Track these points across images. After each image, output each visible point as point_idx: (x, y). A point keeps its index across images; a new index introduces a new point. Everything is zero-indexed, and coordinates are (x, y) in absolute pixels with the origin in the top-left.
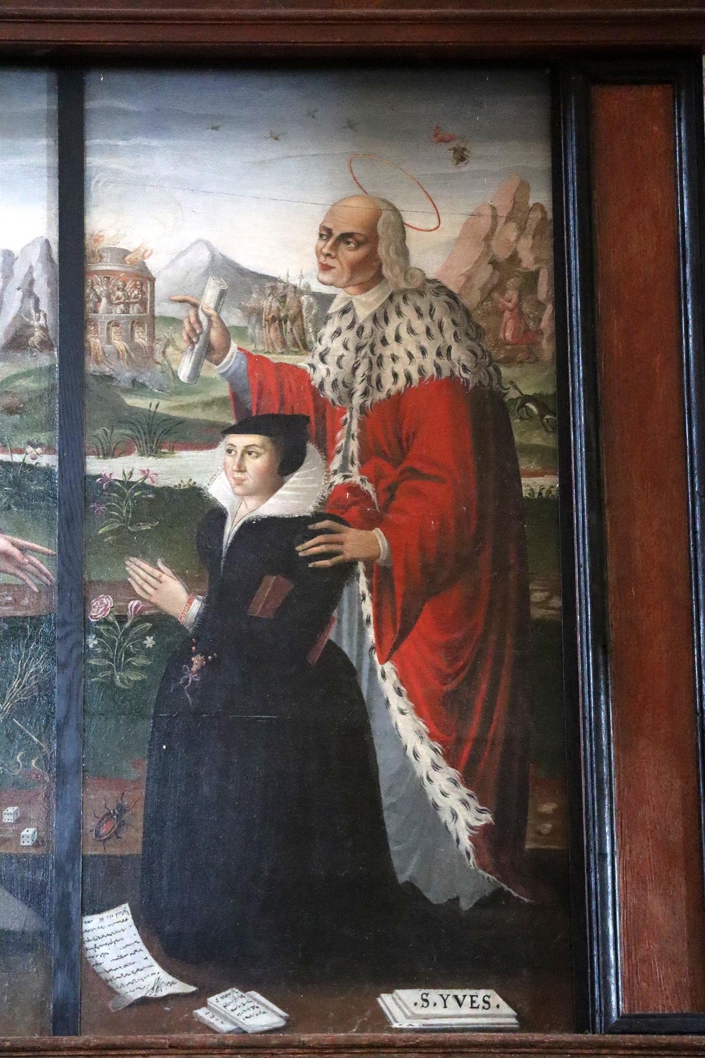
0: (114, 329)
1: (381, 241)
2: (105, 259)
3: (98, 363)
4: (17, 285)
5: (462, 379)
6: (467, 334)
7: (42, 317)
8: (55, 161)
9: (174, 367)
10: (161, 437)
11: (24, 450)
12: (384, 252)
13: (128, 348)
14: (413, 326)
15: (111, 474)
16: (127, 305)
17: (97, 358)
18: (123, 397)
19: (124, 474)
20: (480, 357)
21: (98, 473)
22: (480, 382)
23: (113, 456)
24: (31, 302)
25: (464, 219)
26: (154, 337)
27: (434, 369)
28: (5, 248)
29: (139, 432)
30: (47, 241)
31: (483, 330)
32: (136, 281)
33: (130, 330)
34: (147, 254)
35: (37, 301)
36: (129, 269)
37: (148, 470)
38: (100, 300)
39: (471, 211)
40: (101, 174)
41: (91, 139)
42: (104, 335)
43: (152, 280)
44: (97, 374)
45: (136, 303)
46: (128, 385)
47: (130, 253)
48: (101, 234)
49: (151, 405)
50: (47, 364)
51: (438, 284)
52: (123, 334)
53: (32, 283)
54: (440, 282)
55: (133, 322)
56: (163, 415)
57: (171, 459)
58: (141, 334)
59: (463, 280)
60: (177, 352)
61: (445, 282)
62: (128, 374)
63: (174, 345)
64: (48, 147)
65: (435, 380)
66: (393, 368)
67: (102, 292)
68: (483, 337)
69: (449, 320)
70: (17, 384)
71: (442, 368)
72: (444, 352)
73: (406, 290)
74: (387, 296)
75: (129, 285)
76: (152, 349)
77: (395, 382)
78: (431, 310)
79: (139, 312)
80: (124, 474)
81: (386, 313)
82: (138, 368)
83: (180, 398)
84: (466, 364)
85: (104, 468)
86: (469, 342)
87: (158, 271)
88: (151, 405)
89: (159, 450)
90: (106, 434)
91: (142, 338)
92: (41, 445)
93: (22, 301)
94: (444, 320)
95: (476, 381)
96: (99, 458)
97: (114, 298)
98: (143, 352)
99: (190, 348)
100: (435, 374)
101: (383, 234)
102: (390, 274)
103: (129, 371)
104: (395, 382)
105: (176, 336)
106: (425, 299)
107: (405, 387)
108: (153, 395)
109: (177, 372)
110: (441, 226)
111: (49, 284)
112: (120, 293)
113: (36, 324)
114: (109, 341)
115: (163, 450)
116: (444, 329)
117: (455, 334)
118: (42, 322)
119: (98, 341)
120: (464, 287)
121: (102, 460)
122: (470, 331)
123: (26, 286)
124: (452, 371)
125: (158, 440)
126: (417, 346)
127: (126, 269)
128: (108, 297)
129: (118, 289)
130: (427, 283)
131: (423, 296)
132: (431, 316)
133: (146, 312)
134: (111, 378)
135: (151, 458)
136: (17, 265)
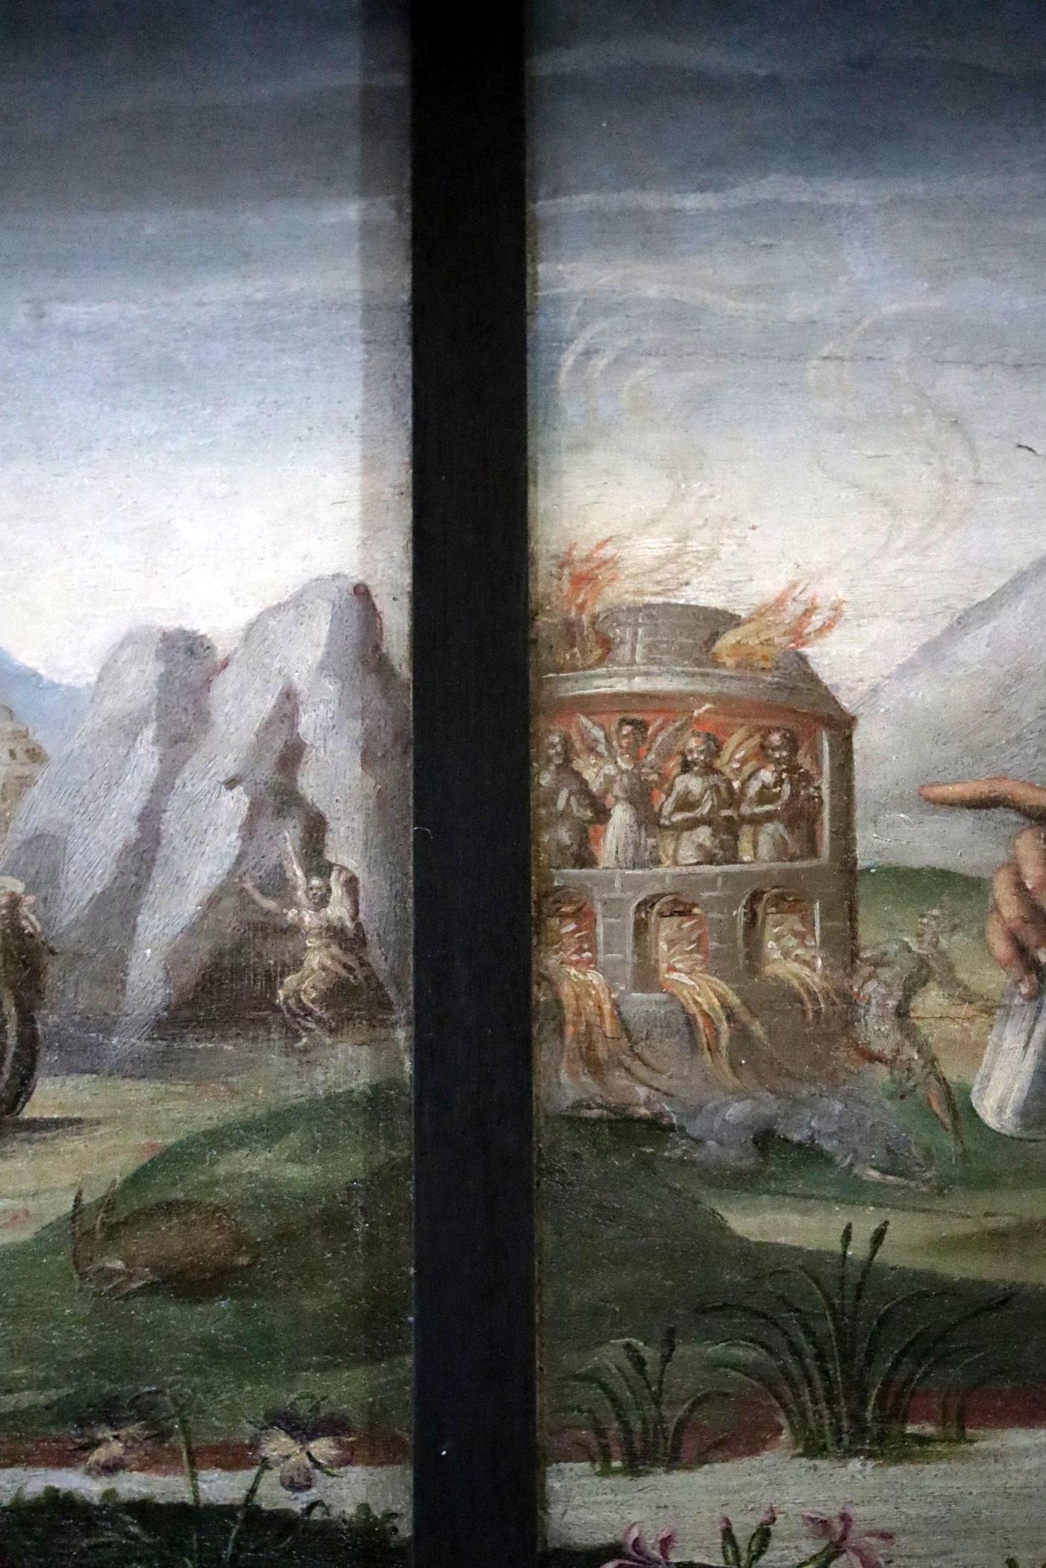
0: (666, 929)
2: (624, 652)
3: (596, 1067)
4: (228, 764)
7: (337, 891)
8: (398, 282)
9: (952, 1072)
10: (900, 1377)
11: (255, 1446)
13: (734, 1000)
15: (666, 1543)
16: (729, 830)
17: (591, 1047)
18: (712, 1202)
19: (728, 1534)
21: (603, 1537)
23: (674, 1461)
24: (289, 837)
26: (854, 955)
28: (171, 624)
29: (796, 1352)
30: (362, 592)
32: (769, 731)
33: (740, 933)
34: (817, 621)
35: (315, 829)
36: (734, 688)
37: (845, 1518)
38: (602, 814)
40: (601, 324)
41: (555, 193)
42: (626, 952)
43: (842, 726)
44: (595, 1113)
45: (769, 817)
46: (738, 1156)
47: (732, 621)
48: (608, 551)
49: (847, 1235)
50: (361, 1081)
52: (713, 944)
53: (292, 757)
55: (756, 896)
56: (902, 1273)
57: (955, 1465)
58: (794, 942)
60: (965, 1010)
62: (736, 1111)
63: (950, 980)
64: (368, 230)
67: (610, 780)
70: (221, 1170)
75: (737, 748)
76: (848, 1005)
79: (782, 851)
80: (728, 1534)
82: (783, 1083)
83: (983, 1202)
85: (635, 1516)
87: (863, 687)
88: (847, 1235)
89: (895, 1429)
90: (640, 1363)
91: (797, 958)
92: (334, 1426)
93: (249, 829)
96: (606, 1472)
97: (666, 804)
98: (804, 1013)
99: (1024, 989)
103: (741, 1095)
105: (955, 944)
108: (854, 1192)
109: (967, 1092)
111: (368, 759)
112: (693, 784)
113: (308, 918)
114: (646, 977)
115: (911, 1429)
118: (338, 910)
119: (594, 977)
121: (623, 1481)
123: (266, 771)
125: (887, 1384)
127: (717, 688)
128: (641, 798)
129: (686, 767)
133: (813, 851)
134: (657, 1128)
135: (855, 1464)
136: (225, 686)
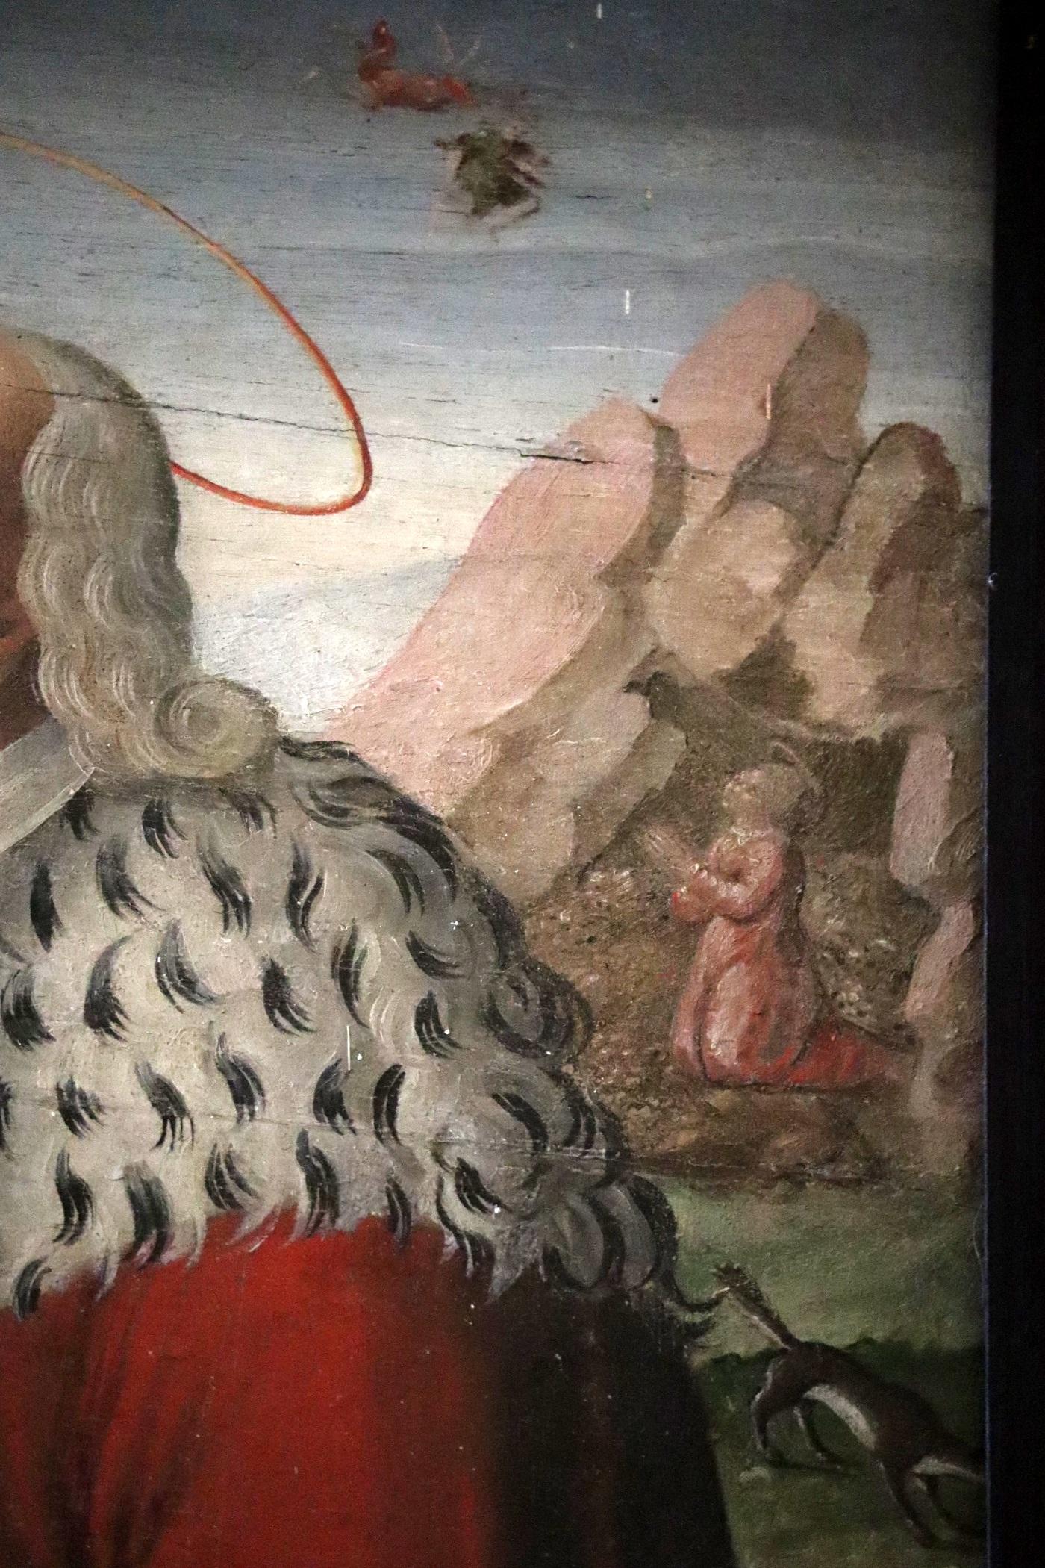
1: (37, 539)
5: (451, 1240)
6: (493, 1020)
12: (52, 593)
14: (195, 960)
20: (557, 1135)
22: (551, 1258)
25: (502, 470)
27: (300, 1177)
31: (583, 1003)
39: (544, 435)
51: (341, 768)
54: (352, 757)
59: (483, 756)
61: (382, 760)
65: (299, 1228)
66: (62, 1158)
68: (579, 1038)
69: (397, 943)
71: (343, 1179)
72: (357, 1097)
73: (162, 783)
74: (56, 804)
77: (72, 1230)
78: (295, 888)
81: (42, 883)
84: (474, 1160)
86: (503, 1058)
94: (368, 939)
95: (532, 1251)
100: (304, 1203)
101: (51, 503)
102: (80, 702)
104: (72, 1230)
106: (268, 829)
107: (128, 1255)
110: (372, 494)
116: (364, 983)
117: (426, 1014)
120: (489, 788)
122: (510, 1005)
124: (398, 1198)
126: (206, 1057)
130: (279, 755)
131: (256, 816)
132: (298, 914)
